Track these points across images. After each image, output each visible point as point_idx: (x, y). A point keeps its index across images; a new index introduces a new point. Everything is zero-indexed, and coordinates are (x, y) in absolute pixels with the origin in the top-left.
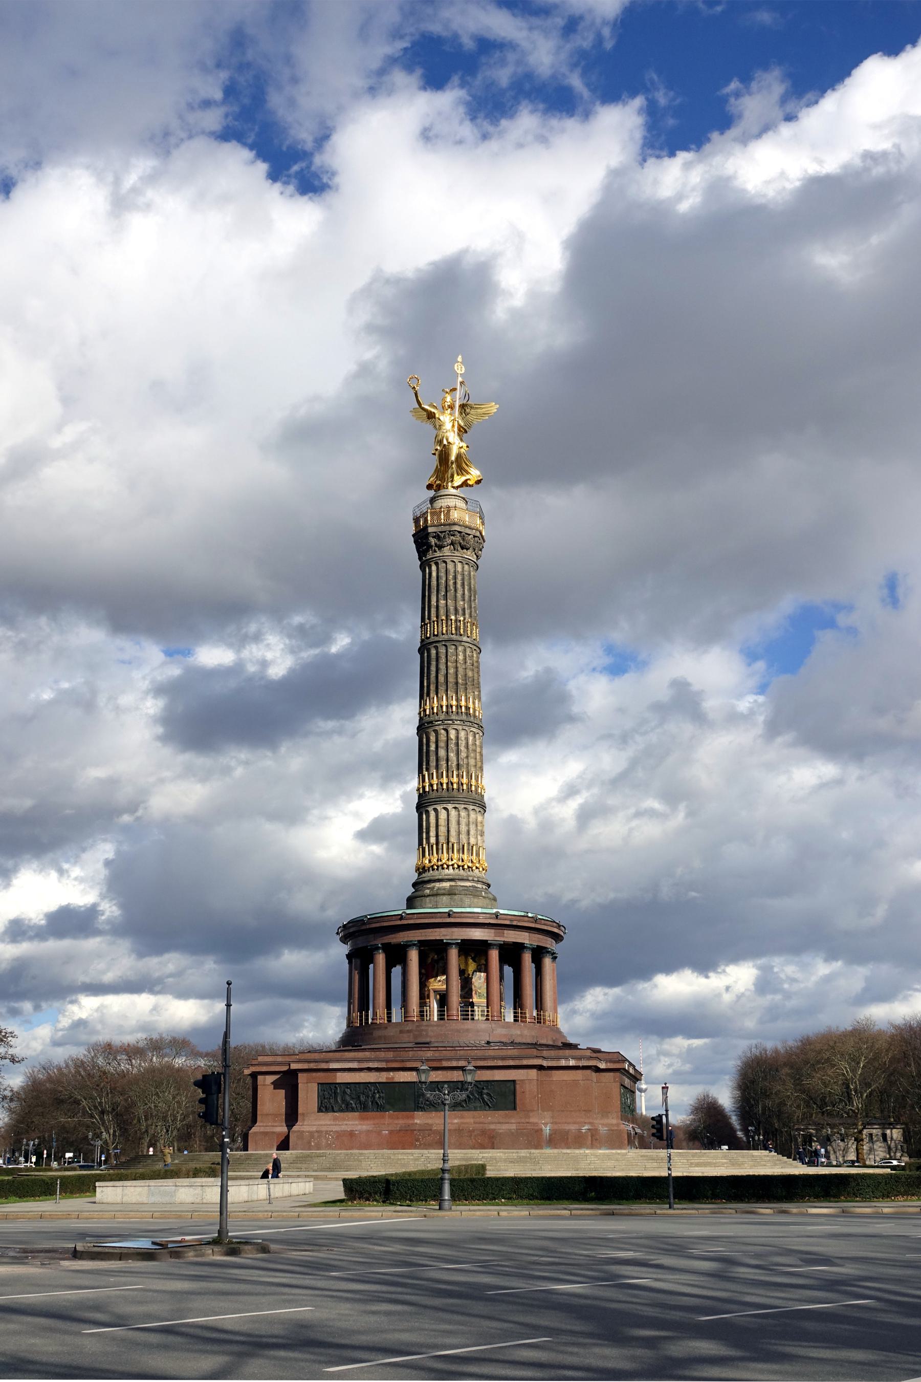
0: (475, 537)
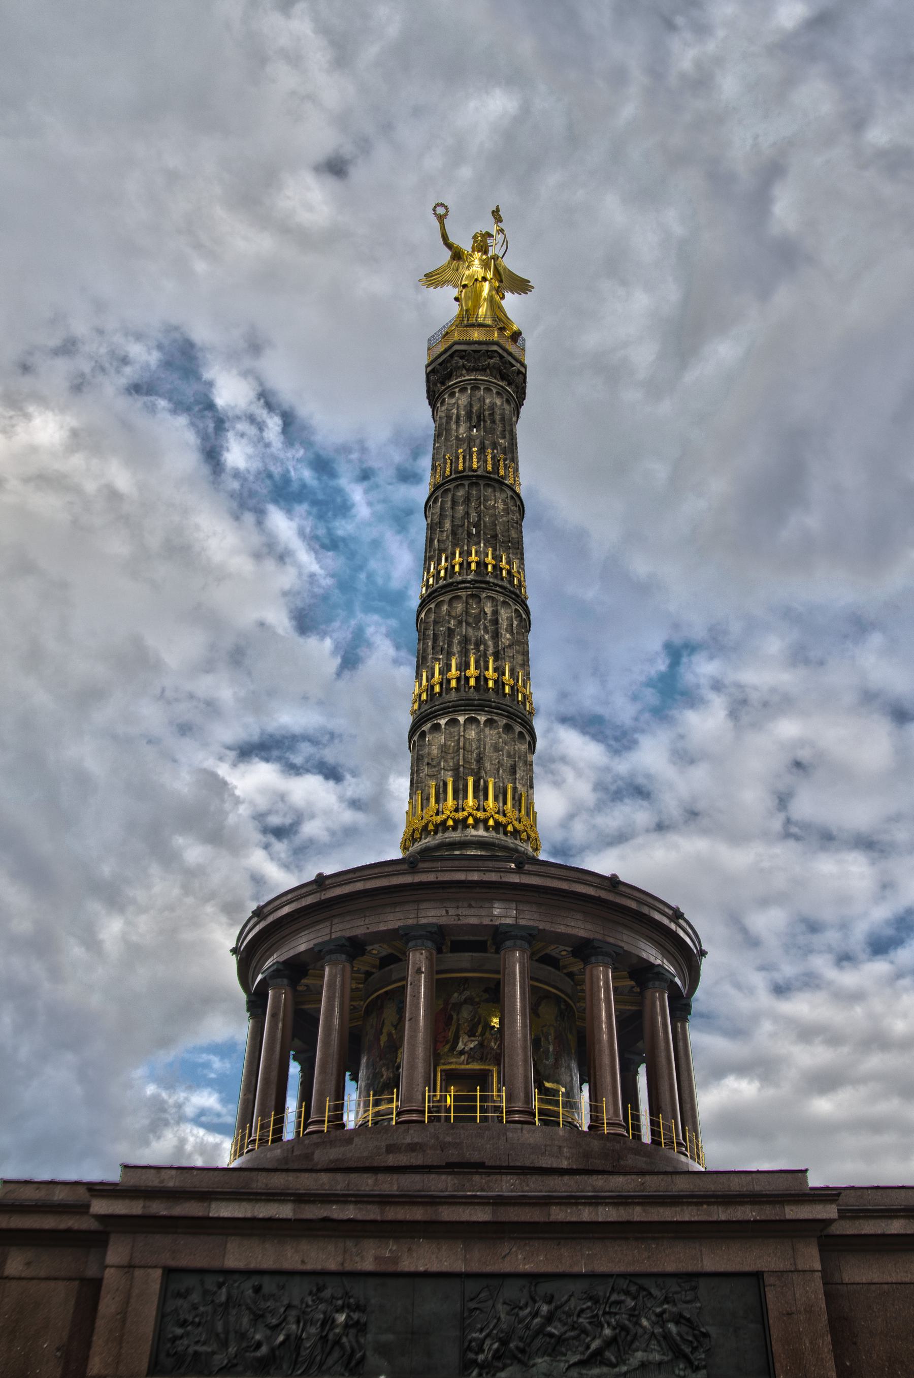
0: (519, 372)
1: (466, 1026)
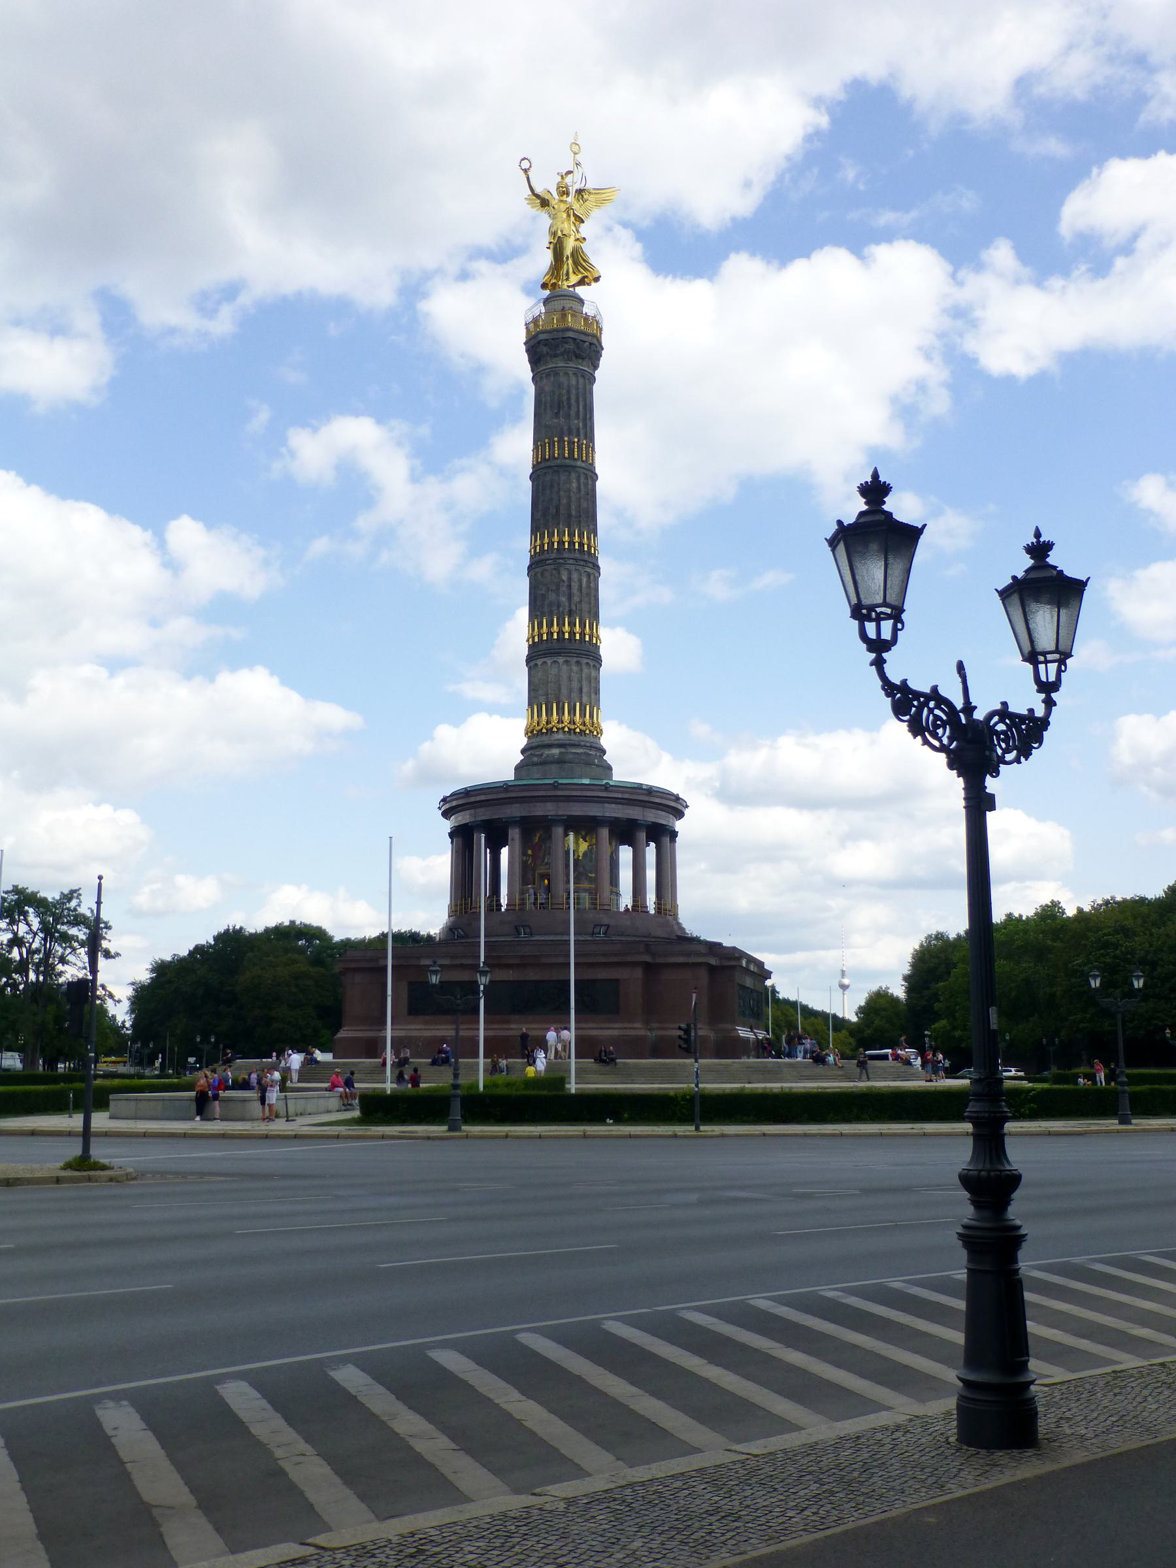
0: (591, 344)
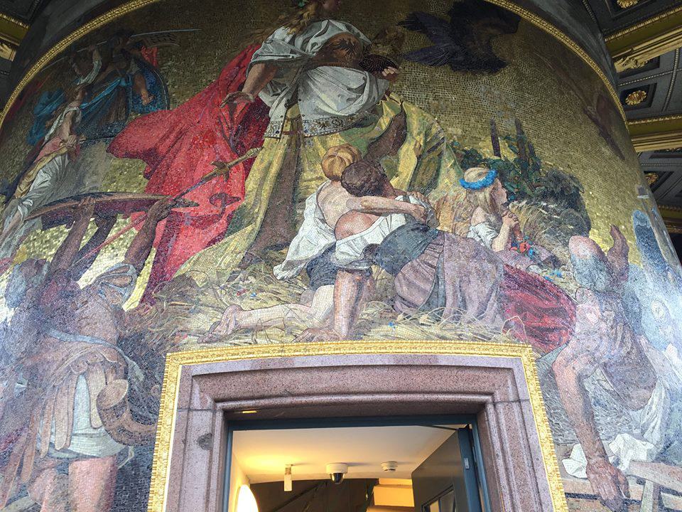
1: (333, 149)
